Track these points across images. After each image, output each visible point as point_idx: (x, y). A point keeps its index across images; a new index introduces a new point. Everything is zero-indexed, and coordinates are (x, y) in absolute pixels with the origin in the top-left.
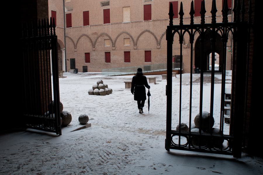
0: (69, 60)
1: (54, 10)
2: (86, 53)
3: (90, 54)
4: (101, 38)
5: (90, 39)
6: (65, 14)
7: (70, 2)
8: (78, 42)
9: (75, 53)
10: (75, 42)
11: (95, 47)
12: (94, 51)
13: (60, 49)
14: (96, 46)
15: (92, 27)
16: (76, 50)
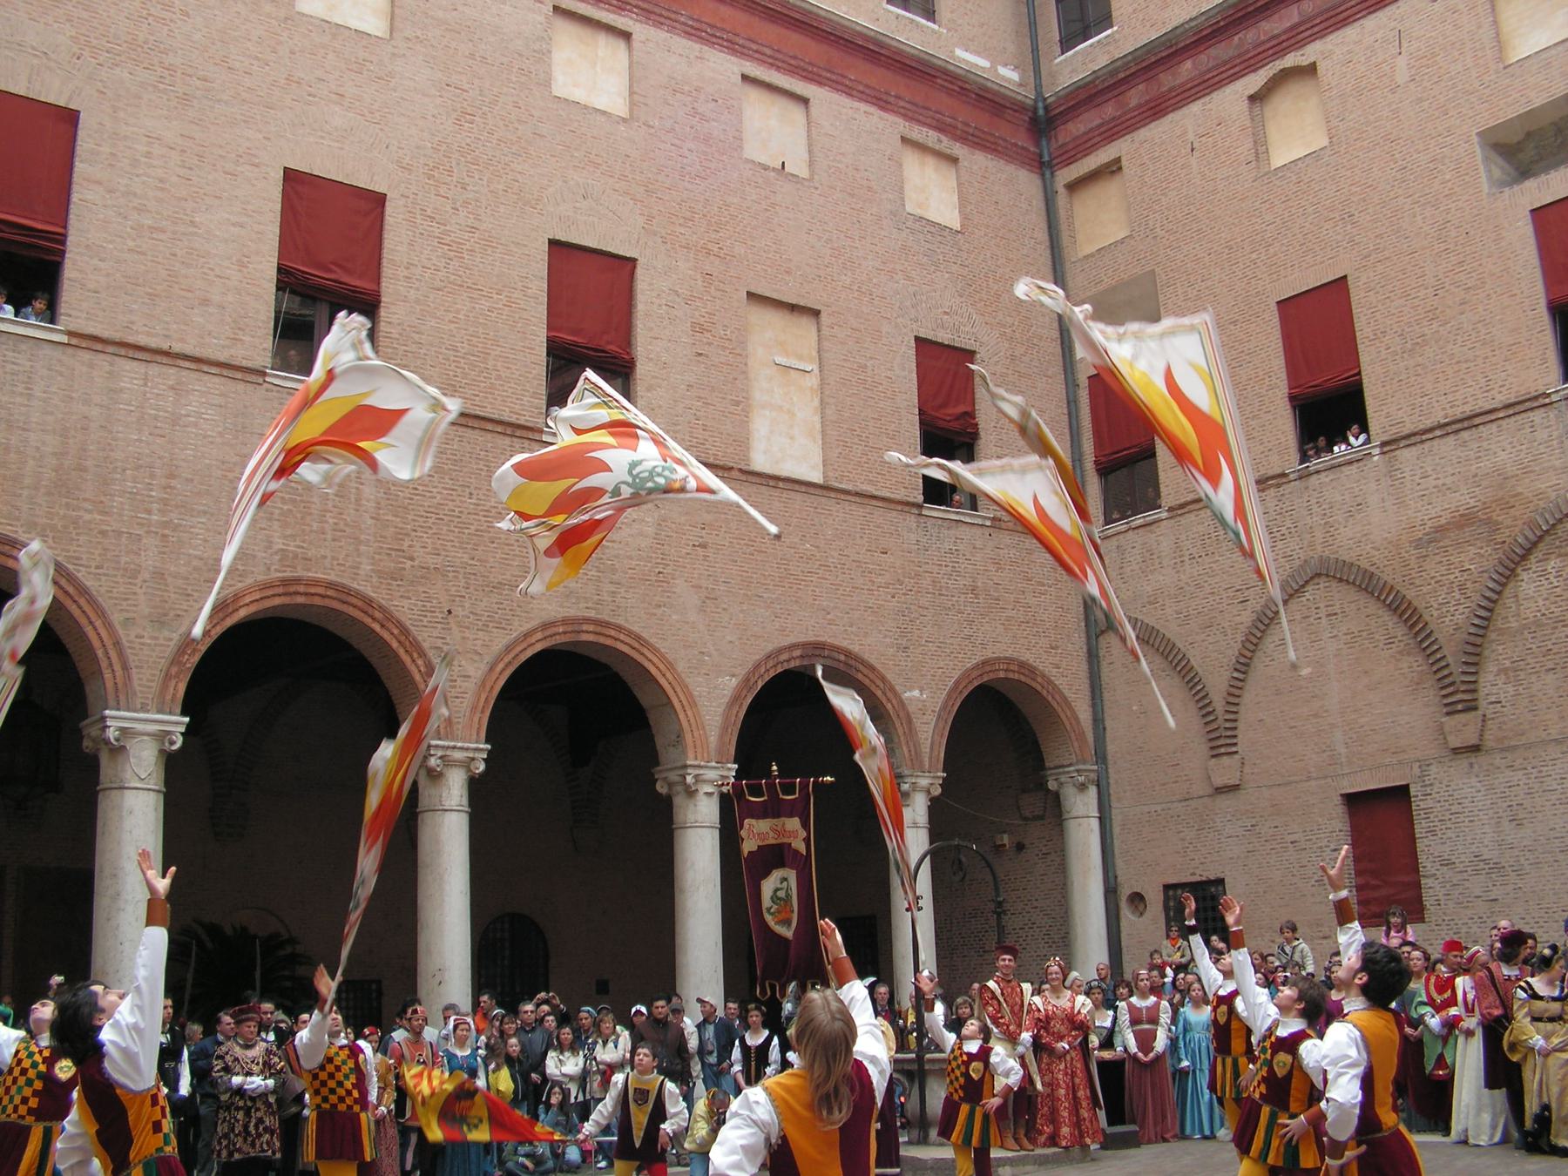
0: (1155, 898)
1: (943, 337)
2: (1355, 802)
3: (1419, 803)
4: (1553, 564)
5: (1405, 611)
6: (1083, 380)
7: (1122, 241)
8: (1243, 666)
9: (1224, 802)
10: (1217, 682)
11: (1471, 707)
12: (1463, 762)
13: (1041, 785)
14: (1492, 685)
15: (1406, 455)
16: (1225, 772)
